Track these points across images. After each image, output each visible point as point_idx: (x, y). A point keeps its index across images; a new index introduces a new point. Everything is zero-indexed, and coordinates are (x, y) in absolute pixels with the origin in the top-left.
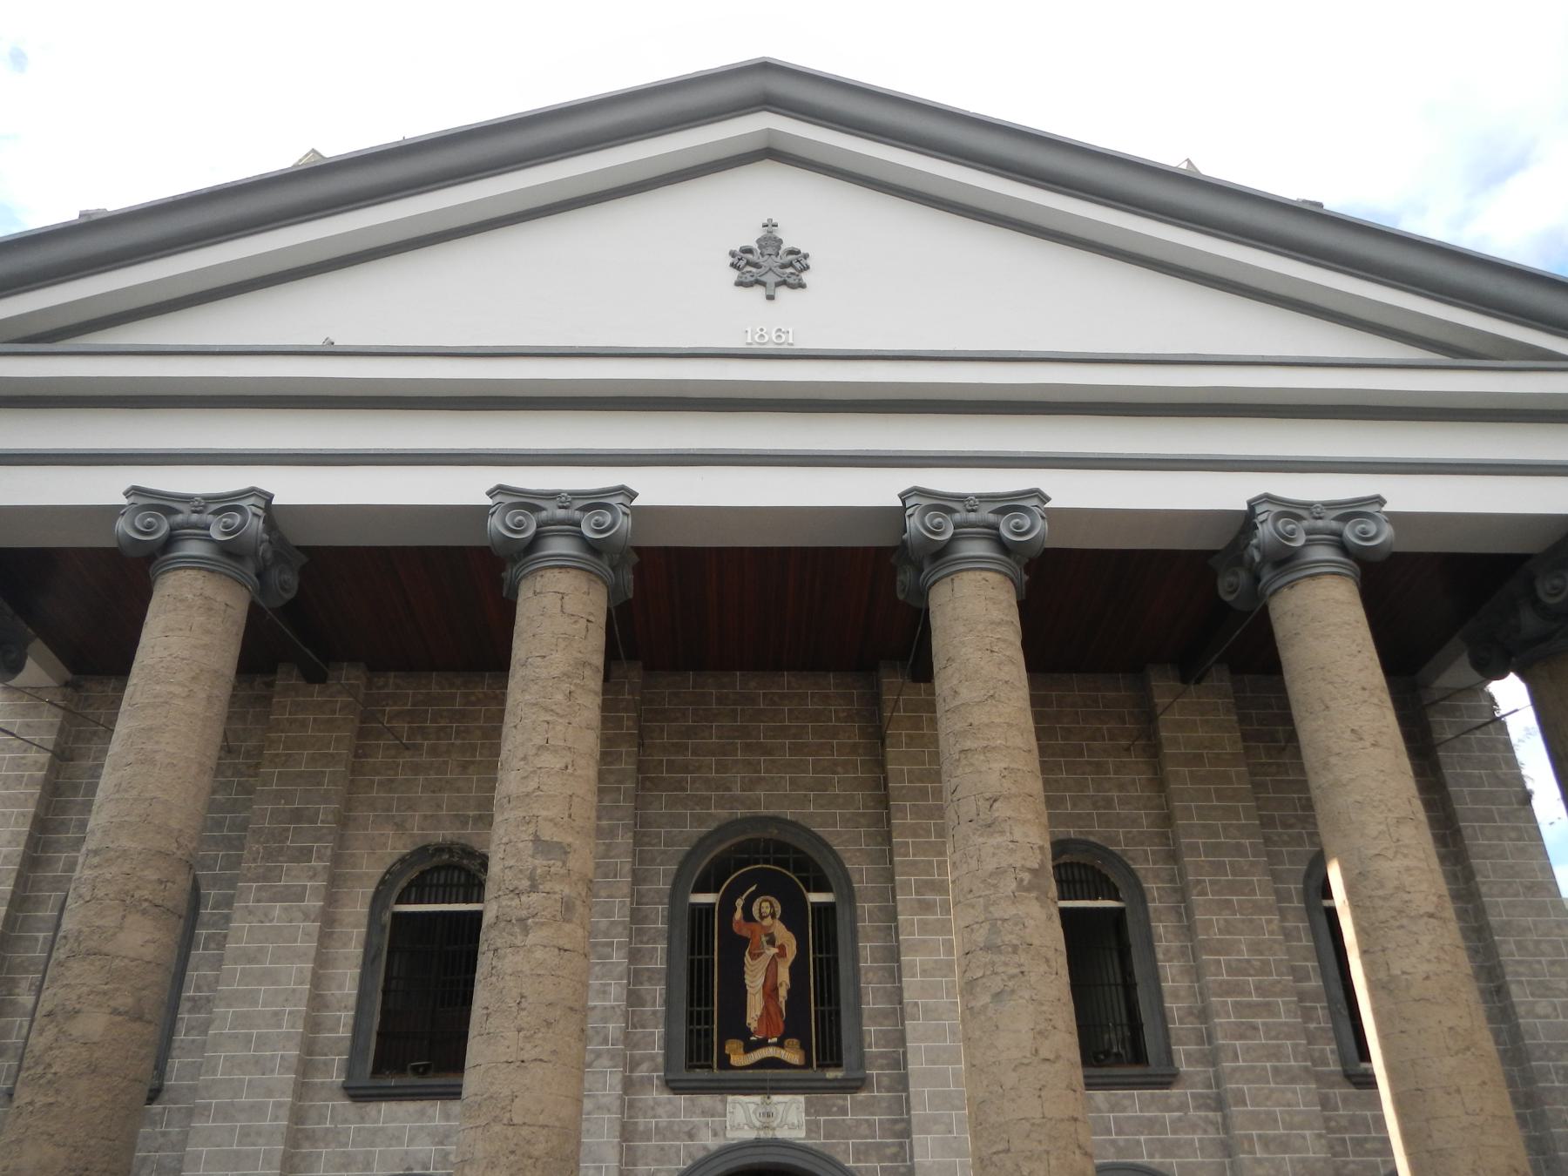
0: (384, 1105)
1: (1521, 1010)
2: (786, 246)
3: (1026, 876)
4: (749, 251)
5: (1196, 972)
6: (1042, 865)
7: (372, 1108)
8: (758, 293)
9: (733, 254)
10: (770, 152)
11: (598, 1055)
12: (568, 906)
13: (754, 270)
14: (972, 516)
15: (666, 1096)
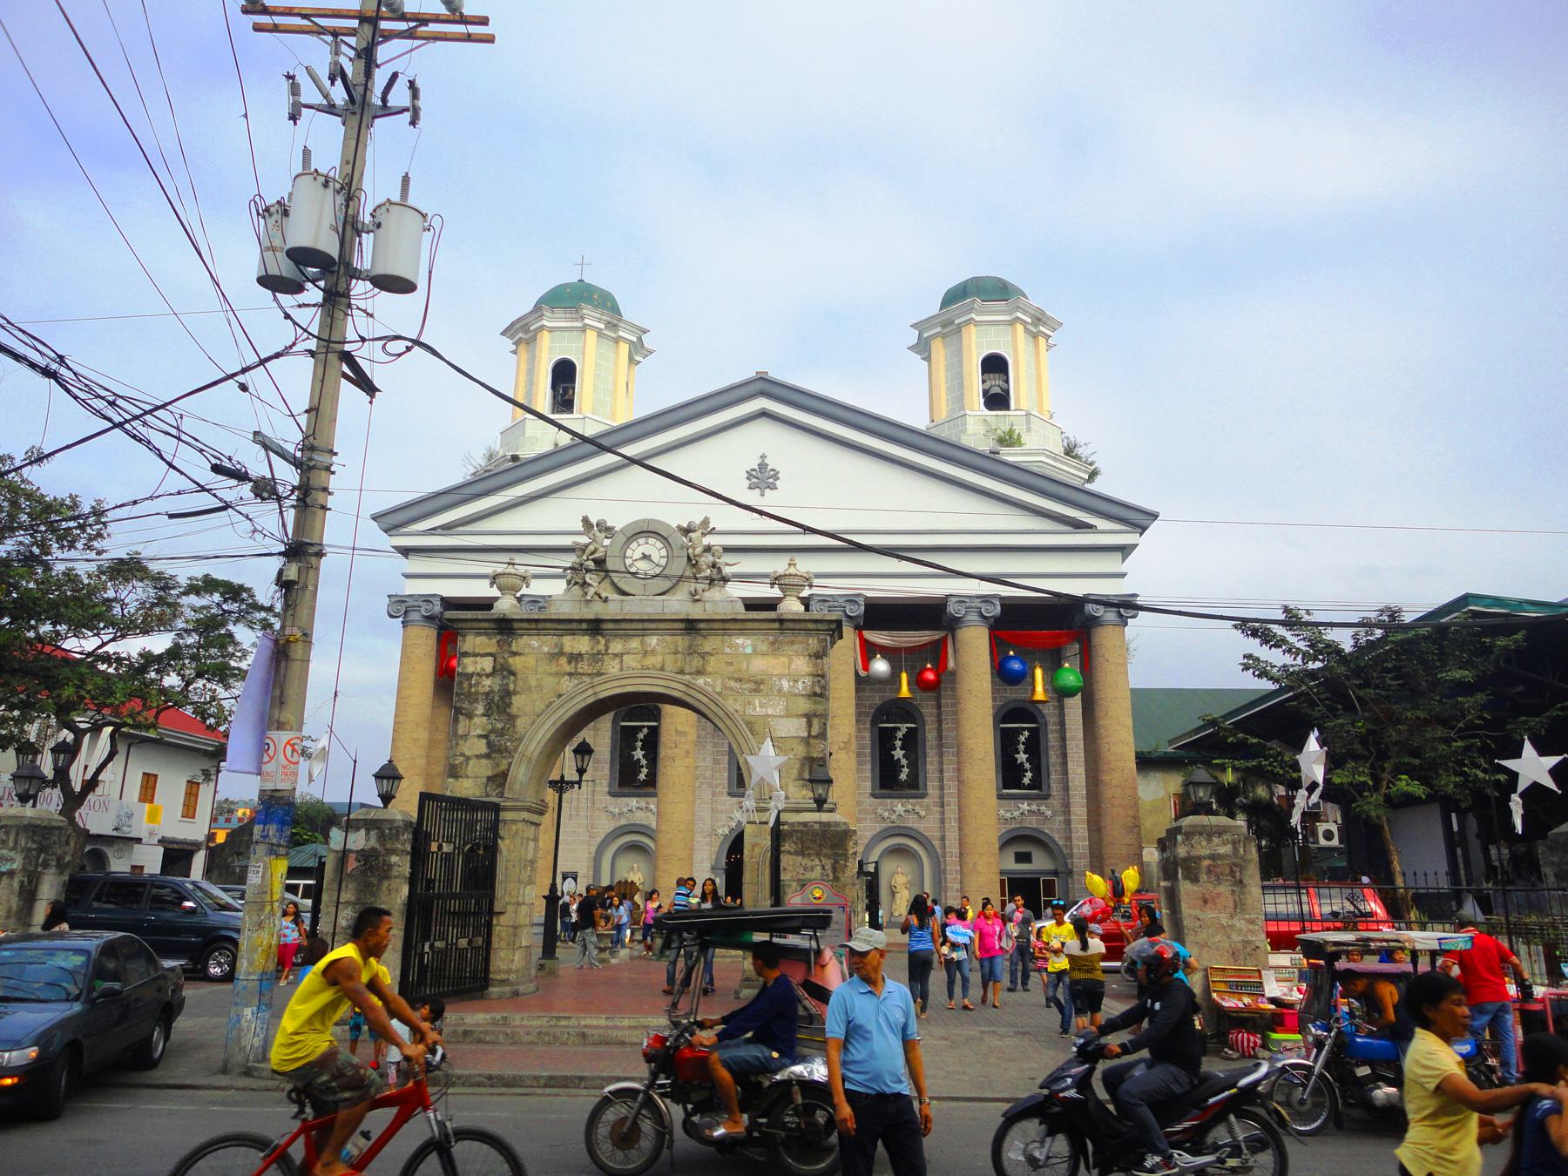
0: (624, 799)
1: (1070, 771)
2: (769, 468)
3: (842, 745)
4: (754, 470)
5: (941, 755)
6: (850, 740)
7: (620, 799)
8: (758, 491)
9: (747, 472)
10: (764, 414)
11: (703, 783)
12: (687, 752)
13: (756, 480)
14: (836, 604)
15: (729, 798)
